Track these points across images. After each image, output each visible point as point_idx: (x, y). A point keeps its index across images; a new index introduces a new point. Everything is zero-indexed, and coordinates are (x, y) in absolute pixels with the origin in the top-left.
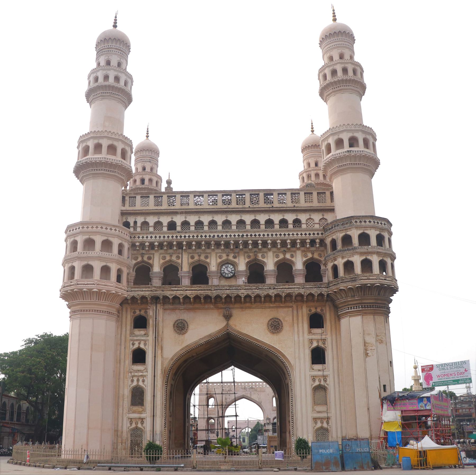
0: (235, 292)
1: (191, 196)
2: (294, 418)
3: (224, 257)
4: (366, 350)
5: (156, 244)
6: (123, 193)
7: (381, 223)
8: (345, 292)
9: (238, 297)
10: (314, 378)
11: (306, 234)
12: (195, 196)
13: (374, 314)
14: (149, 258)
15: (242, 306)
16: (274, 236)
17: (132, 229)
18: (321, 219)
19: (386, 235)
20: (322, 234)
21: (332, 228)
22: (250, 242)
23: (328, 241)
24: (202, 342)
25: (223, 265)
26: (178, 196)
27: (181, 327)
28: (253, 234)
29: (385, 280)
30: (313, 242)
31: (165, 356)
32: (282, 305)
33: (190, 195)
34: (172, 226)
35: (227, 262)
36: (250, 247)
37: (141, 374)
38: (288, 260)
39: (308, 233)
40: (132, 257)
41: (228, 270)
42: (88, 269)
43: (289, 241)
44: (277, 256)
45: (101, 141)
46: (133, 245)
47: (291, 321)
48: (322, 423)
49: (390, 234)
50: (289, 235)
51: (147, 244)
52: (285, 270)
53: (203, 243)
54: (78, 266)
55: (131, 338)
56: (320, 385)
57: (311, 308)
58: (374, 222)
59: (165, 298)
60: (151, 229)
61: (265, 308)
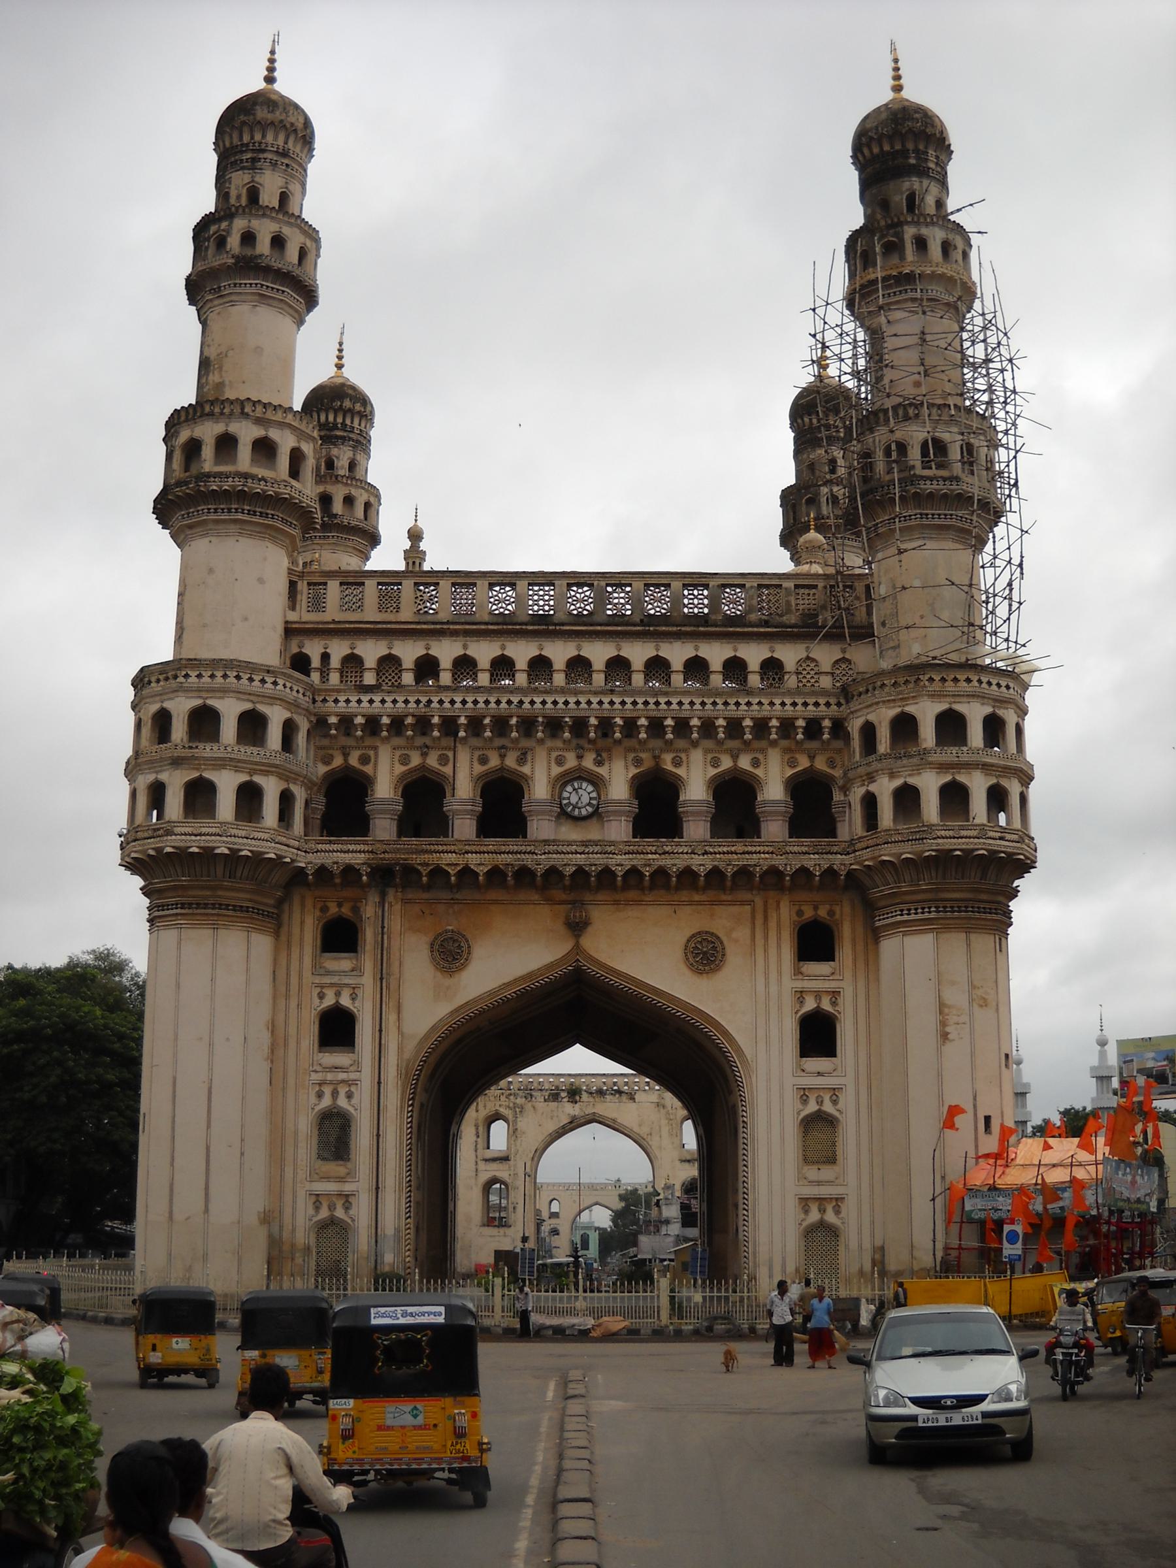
0: (600, 860)
1: (482, 584)
2: (750, 1197)
3: (571, 762)
4: (943, 1024)
5: (385, 720)
6: (290, 572)
7: (999, 685)
8: (896, 869)
9: (607, 874)
10: (804, 1095)
11: (794, 704)
12: (491, 586)
13: (968, 928)
14: (365, 760)
15: (617, 897)
16: (708, 707)
17: (315, 677)
18: (837, 662)
19: (1010, 716)
20: (839, 704)
21: (867, 691)
22: (643, 721)
23: (855, 726)
25: (565, 784)
26: (445, 584)
27: (450, 951)
28: (652, 700)
29: (1001, 838)
30: (813, 728)
31: (407, 1028)
32: (724, 897)
33: (479, 583)
34: (427, 667)
36: (643, 735)
37: (342, 1076)
38: (745, 772)
39: (800, 701)
40: (315, 756)
41: (581, 796)
43: (748, 722)
44: (715, 763)
45: (235, 428)
46: (320, 724)
47: (748, 942)
48: (822, 1211)
49: (1023, 712)
50: (749, 704)
51: (359, 720)
52: (735, 802)
53: (514, 721)
54: (176, 782)
55: (317, 980)
56: (819, 1110)
57: (803, 908)
58: (980, 682)
59: (410, 871)
60: (369, 679)
61: (681, 903)
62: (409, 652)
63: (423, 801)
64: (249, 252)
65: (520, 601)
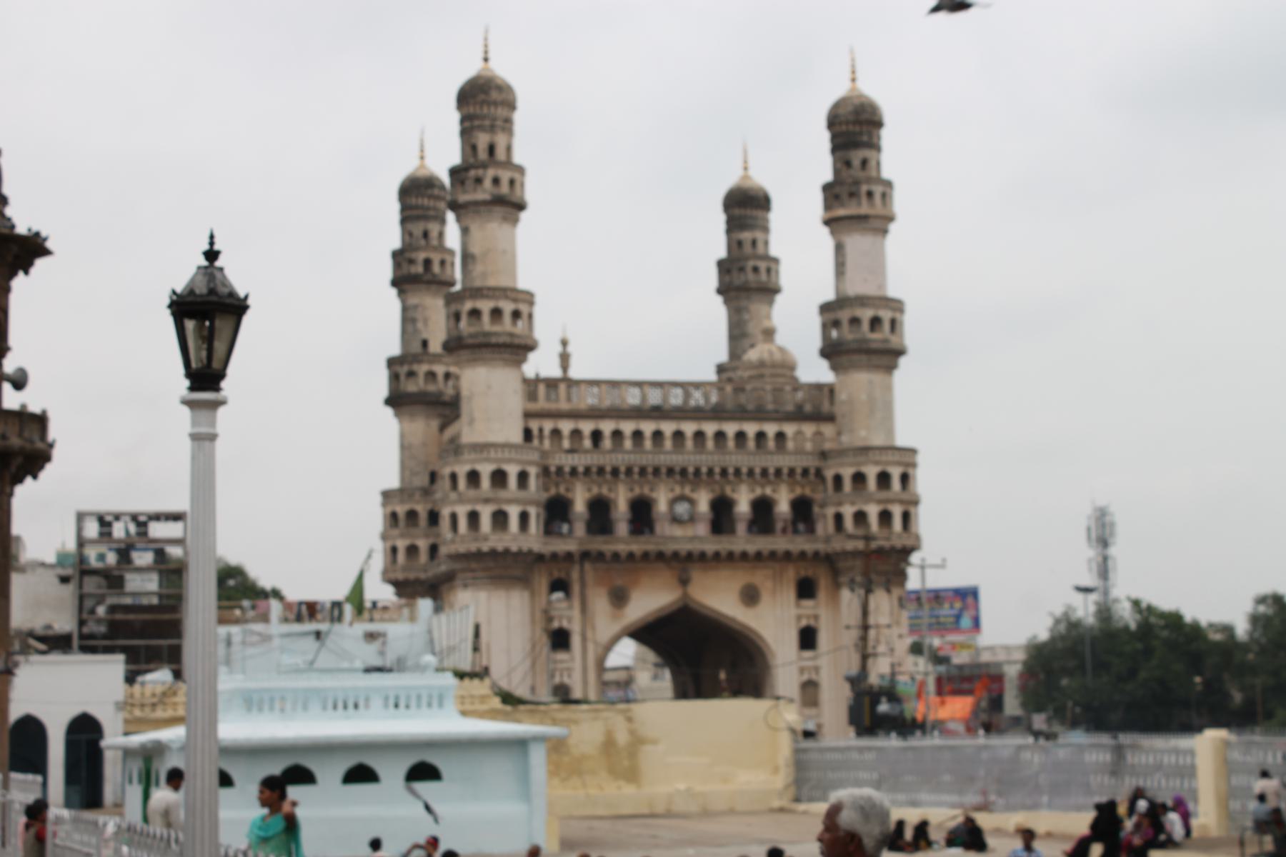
3: (678, 491)
10: (802, 670)
14: (568, 490)
19: (910, 471)
23: (829, 474)
24: (650, 619)
30: (805, 472)
34: (597, 436)
35: (682, 498)
41: (682, 509)
42: (500, 519)
44: (753, 491)
49: (914, 465)
54: (486, 514)
59: (600, 556)
60: (566, 444)
62: (587, 427)
63: (600, 511)
64: (496, 191)
65: (644, 397)
